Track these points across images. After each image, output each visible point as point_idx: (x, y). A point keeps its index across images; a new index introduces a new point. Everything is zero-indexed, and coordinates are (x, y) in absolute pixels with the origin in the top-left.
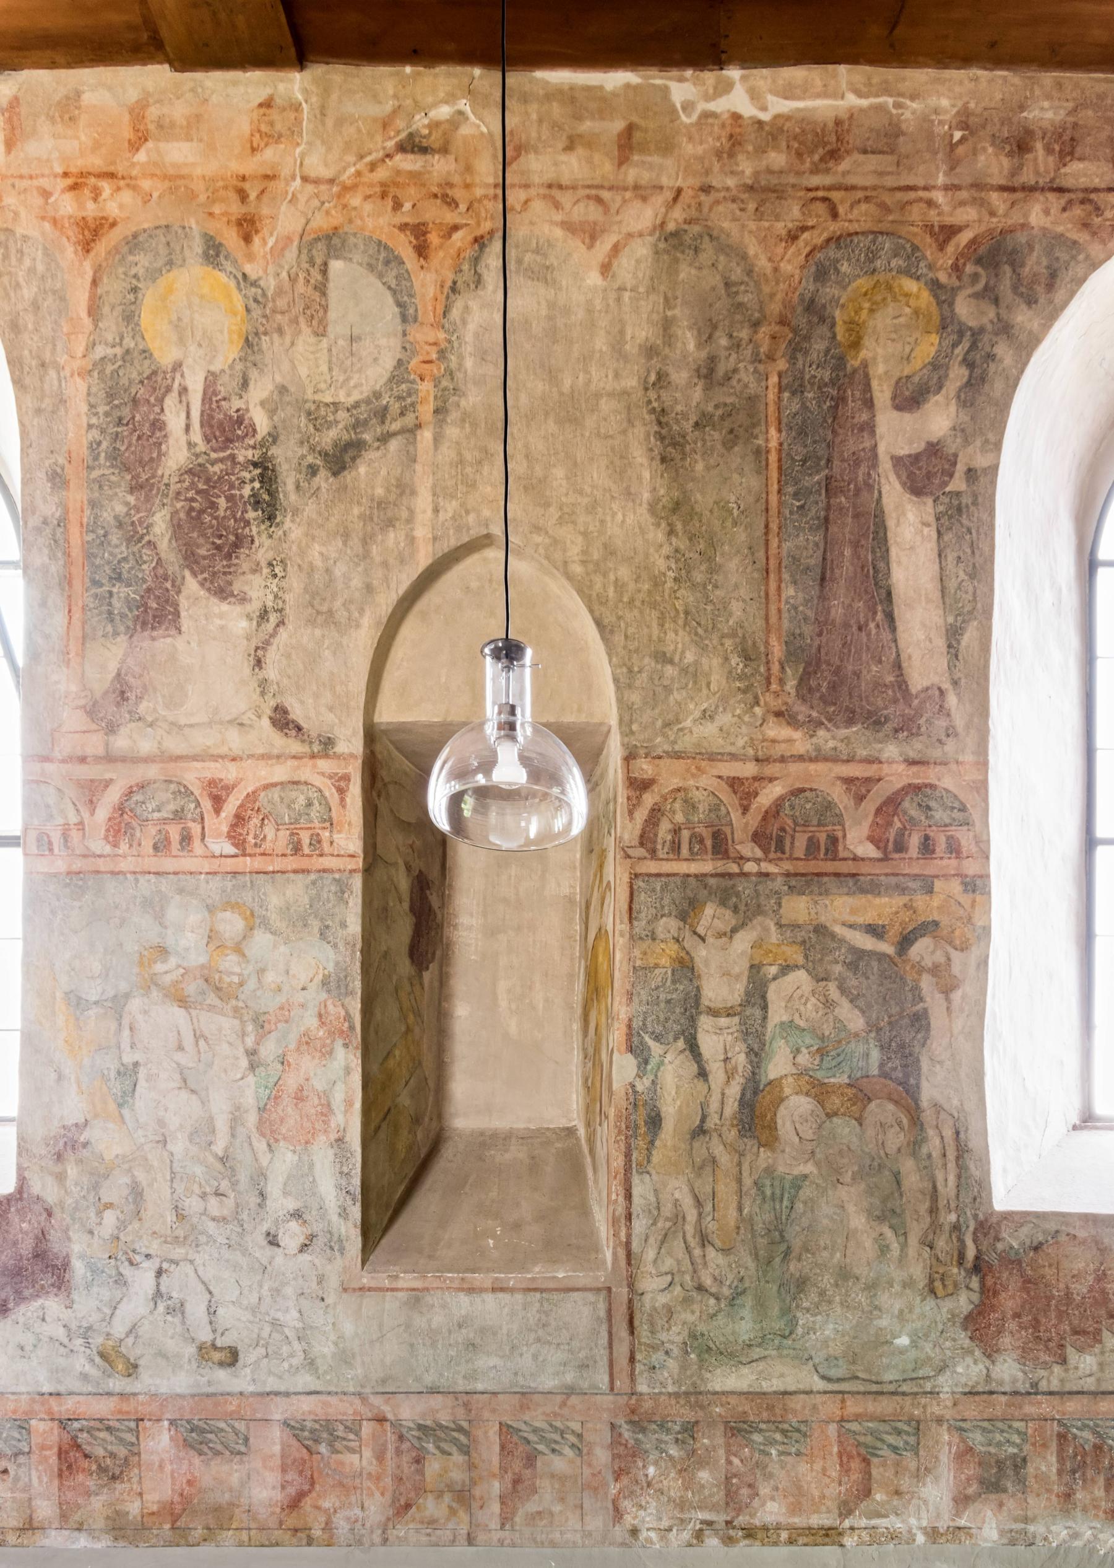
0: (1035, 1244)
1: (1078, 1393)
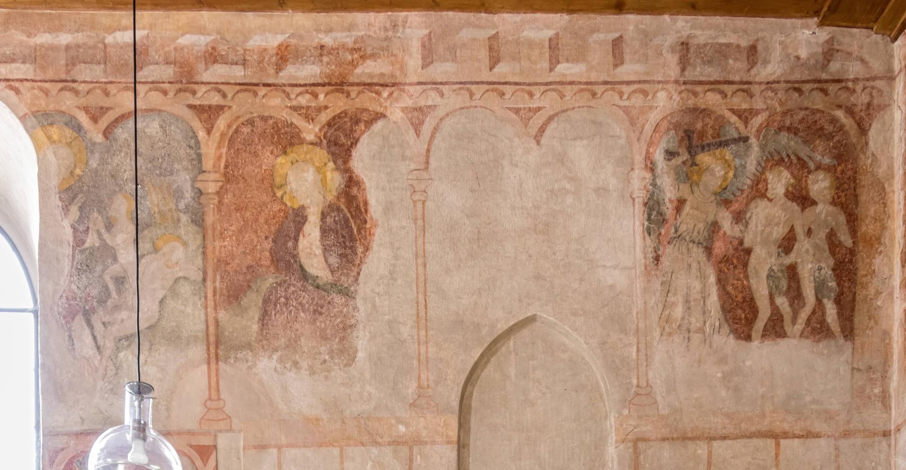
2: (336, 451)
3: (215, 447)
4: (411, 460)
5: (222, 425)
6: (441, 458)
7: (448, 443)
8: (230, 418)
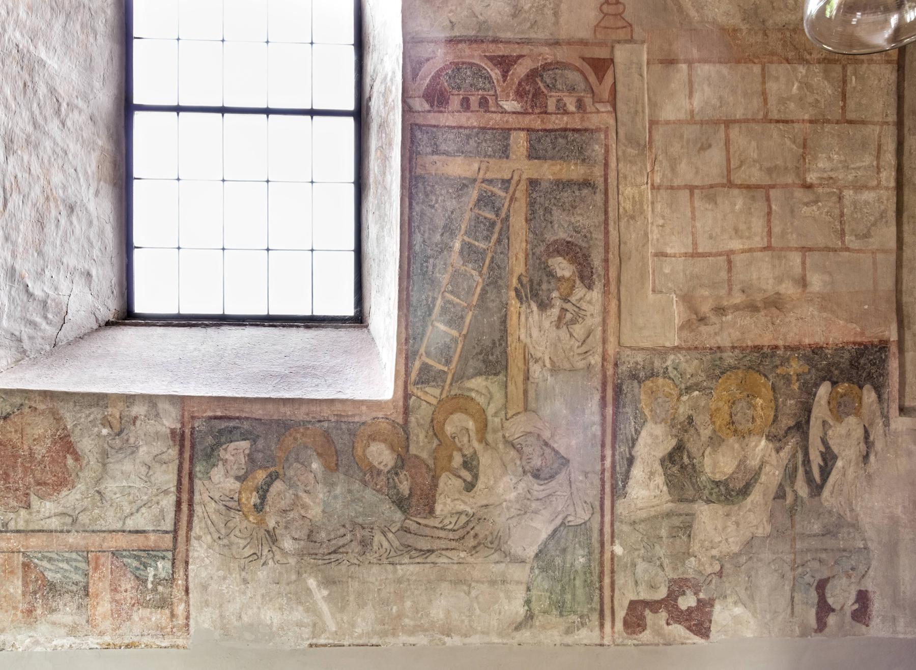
0: (4, 414)
1: (39, 531)
2: (757, 69)
3: (612, 60)
4: (845, 82)
5: (621, 34)
6: (879, 80)
7: (888, 62)
8: (631, 25)
